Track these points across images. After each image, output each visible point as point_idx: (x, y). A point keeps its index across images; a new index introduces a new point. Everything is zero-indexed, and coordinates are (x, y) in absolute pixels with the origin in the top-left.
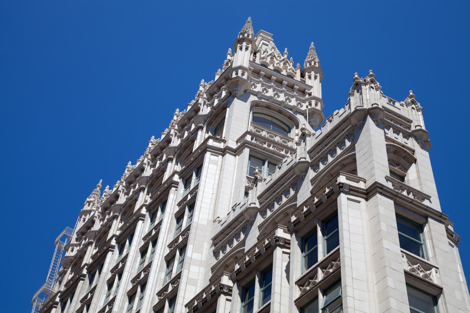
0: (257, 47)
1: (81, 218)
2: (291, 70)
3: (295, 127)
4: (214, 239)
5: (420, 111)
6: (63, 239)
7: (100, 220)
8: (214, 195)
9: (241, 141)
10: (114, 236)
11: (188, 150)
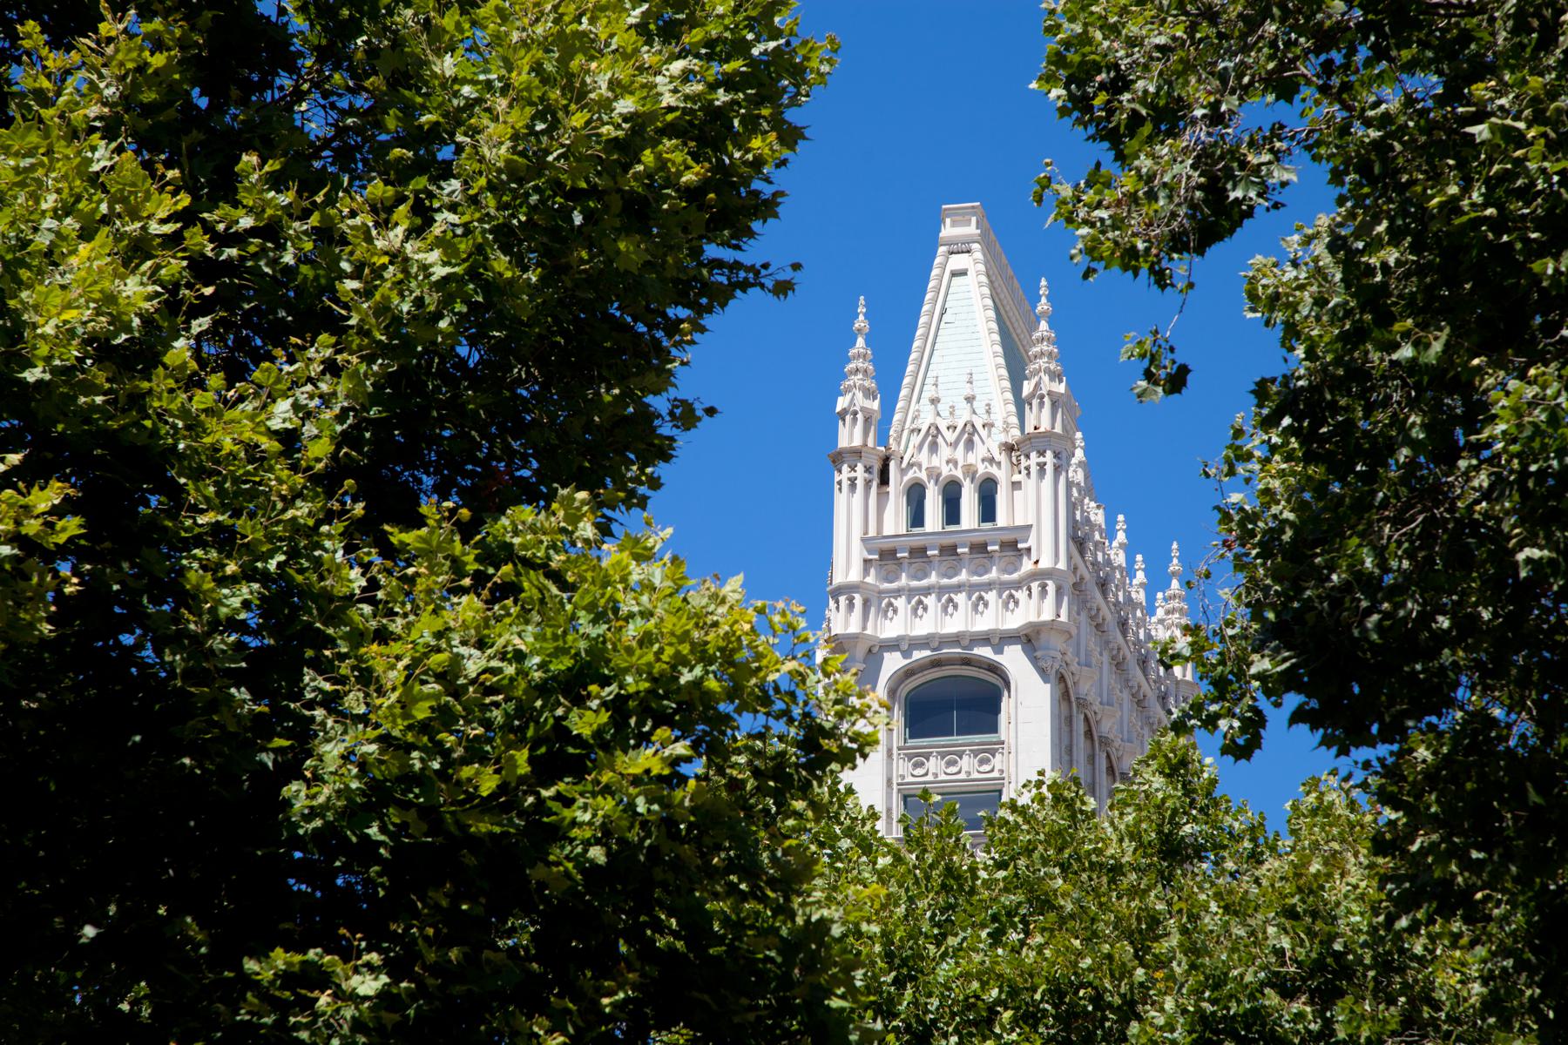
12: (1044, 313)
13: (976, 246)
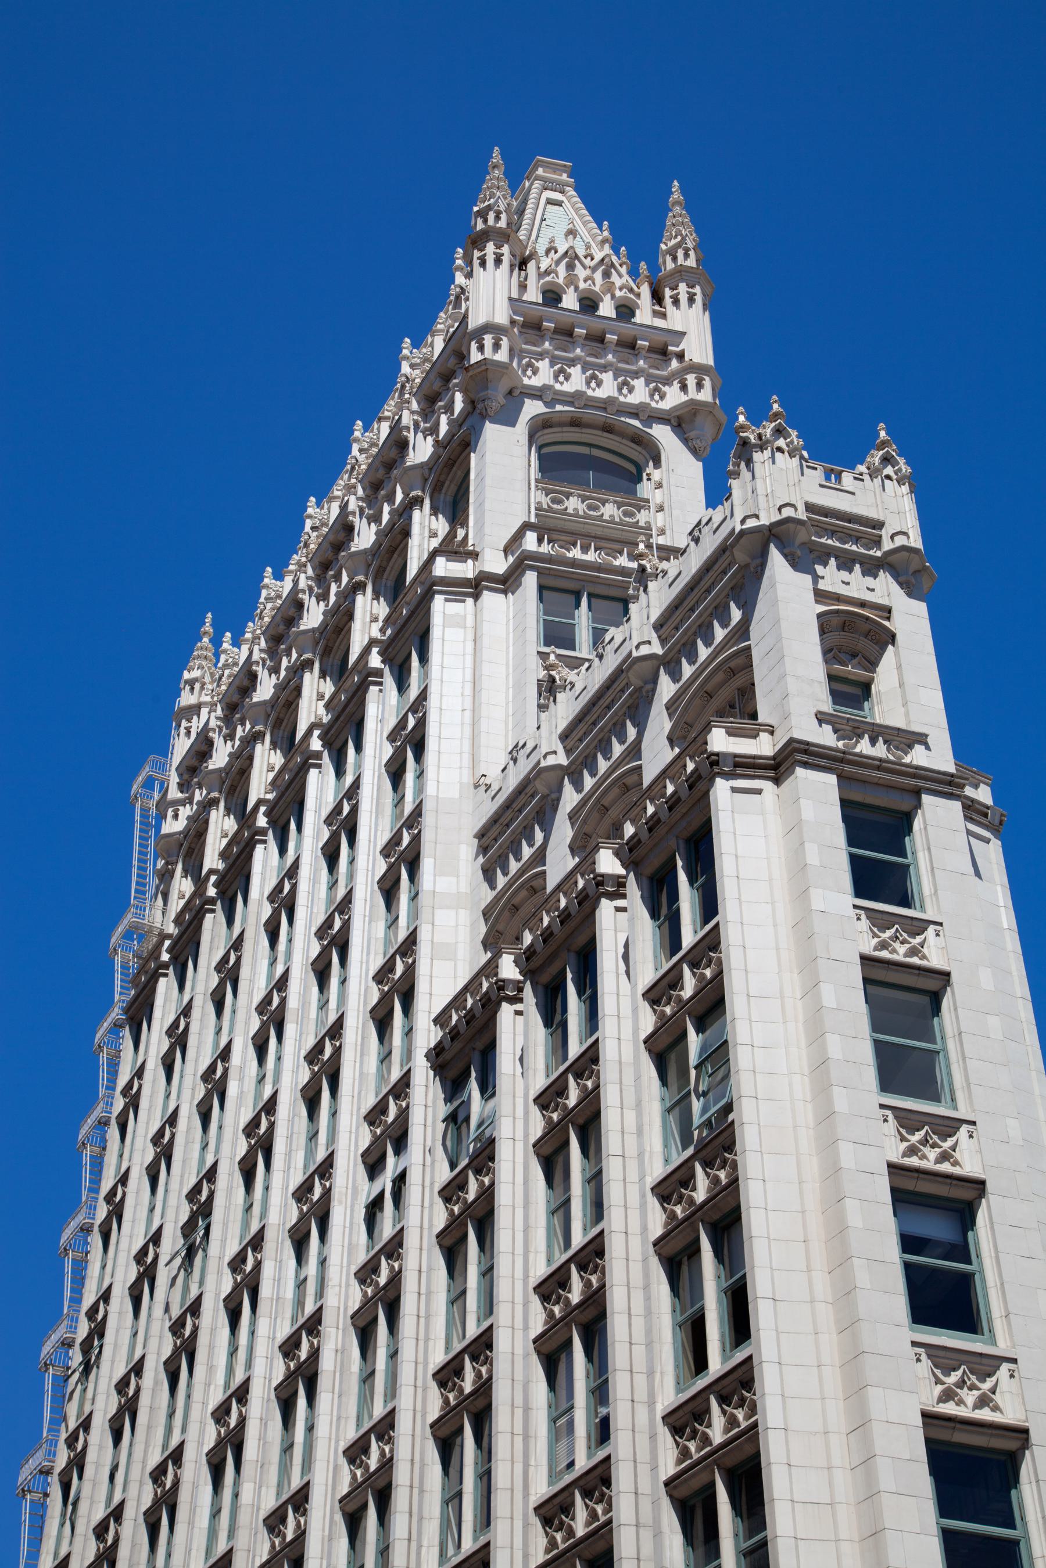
0: (525, 244)
1: (180, 726)
2: (625, 290)
3: (651, 464)
4: (481, 835)
5: (904, 484)
6: (149, 784)
7: (224, 737)
8: (468, 714)
9: (513, 548)
10: (260, 802)
11: (399, 556)
12: (677, 203)
13: (571, 192)
